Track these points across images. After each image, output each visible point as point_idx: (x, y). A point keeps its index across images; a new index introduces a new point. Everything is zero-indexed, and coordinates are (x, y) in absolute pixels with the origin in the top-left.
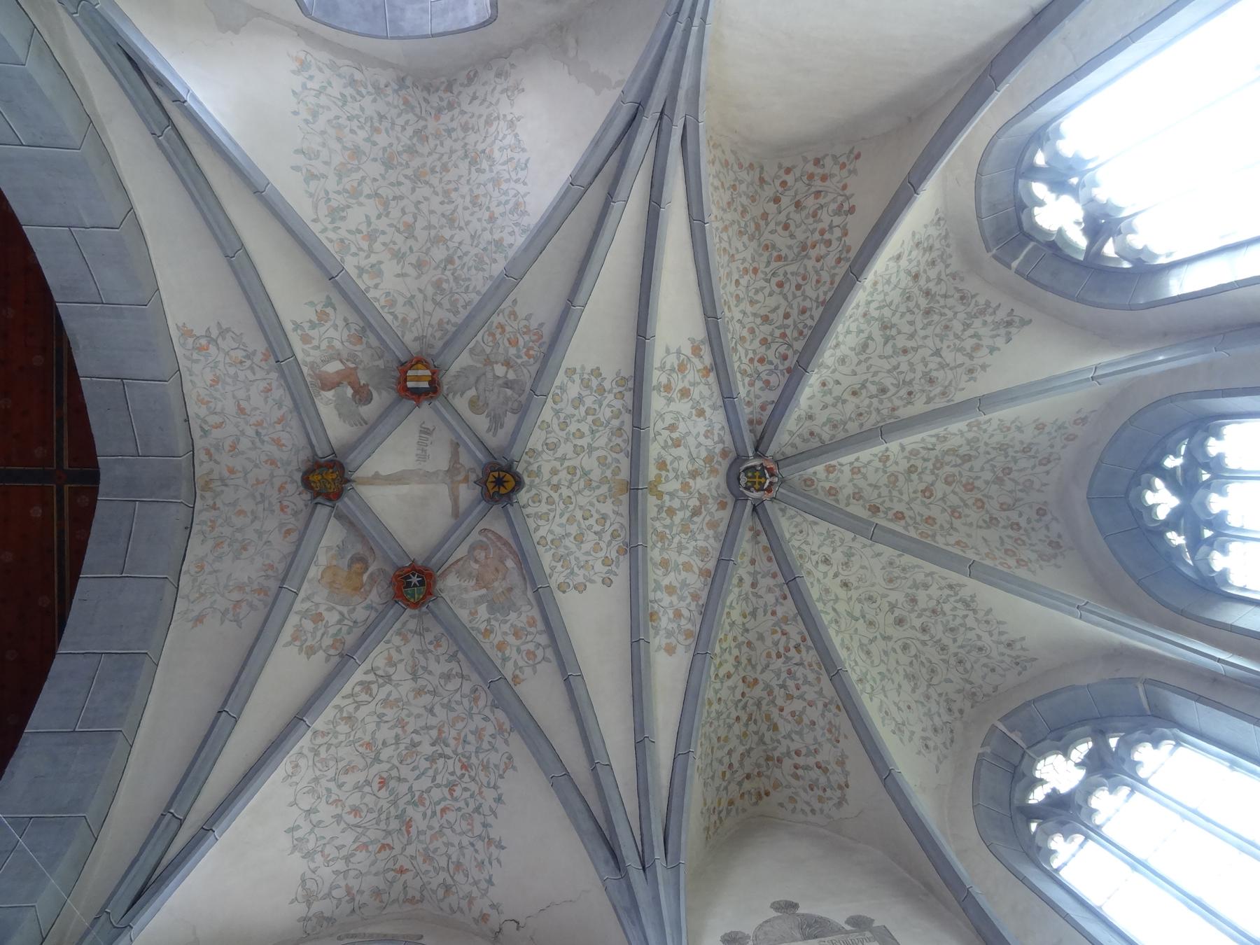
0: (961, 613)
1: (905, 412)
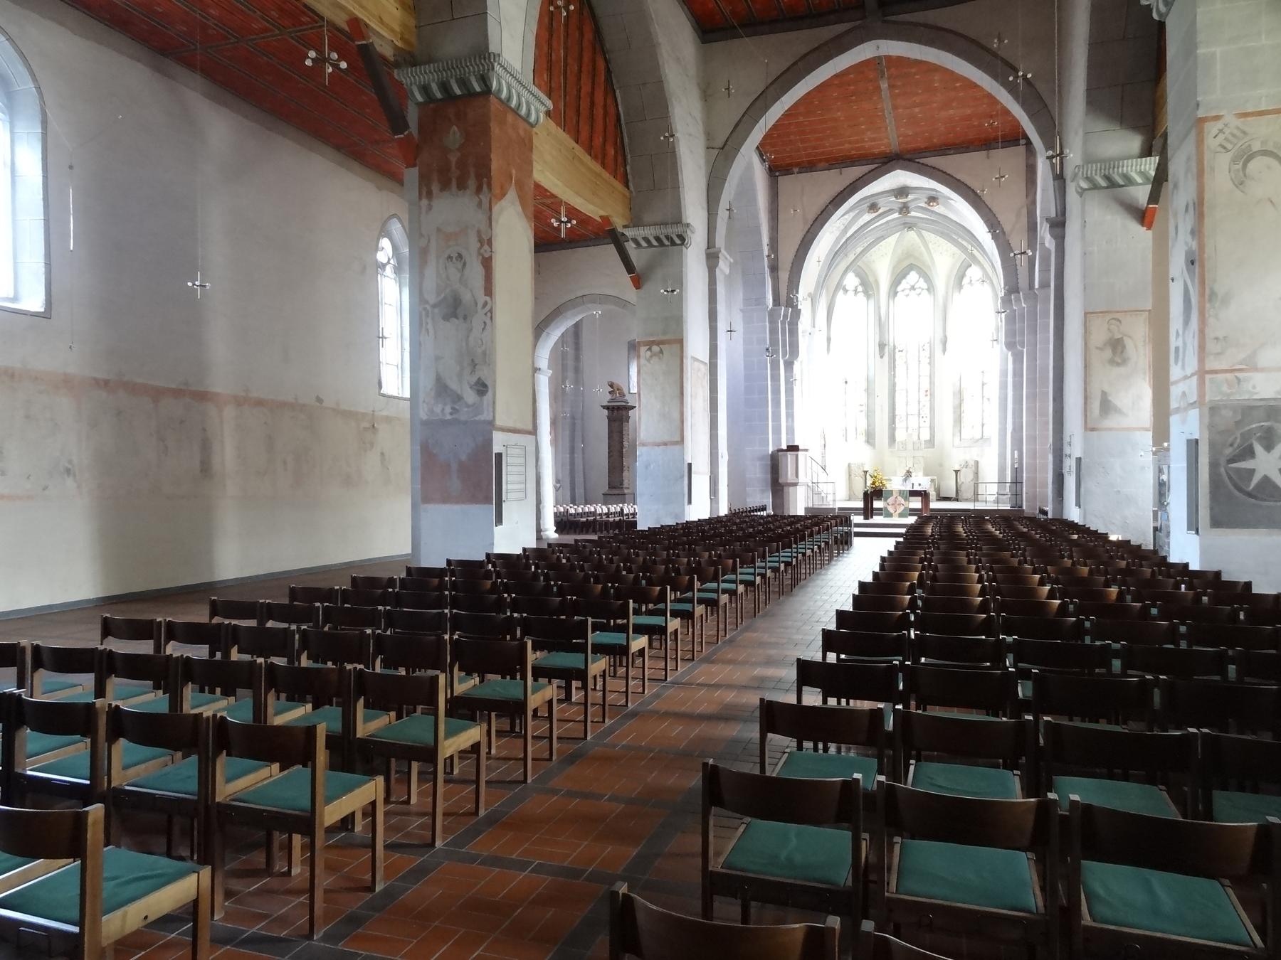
1: (930, 245)
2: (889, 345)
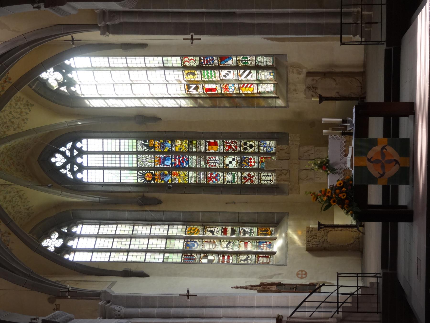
0: (17, 201)
2: (144, 192)
